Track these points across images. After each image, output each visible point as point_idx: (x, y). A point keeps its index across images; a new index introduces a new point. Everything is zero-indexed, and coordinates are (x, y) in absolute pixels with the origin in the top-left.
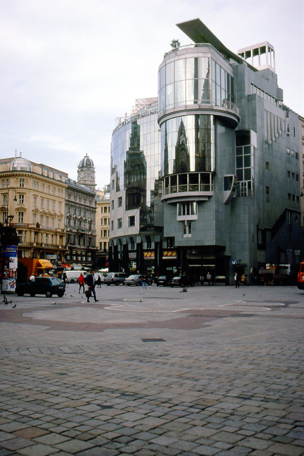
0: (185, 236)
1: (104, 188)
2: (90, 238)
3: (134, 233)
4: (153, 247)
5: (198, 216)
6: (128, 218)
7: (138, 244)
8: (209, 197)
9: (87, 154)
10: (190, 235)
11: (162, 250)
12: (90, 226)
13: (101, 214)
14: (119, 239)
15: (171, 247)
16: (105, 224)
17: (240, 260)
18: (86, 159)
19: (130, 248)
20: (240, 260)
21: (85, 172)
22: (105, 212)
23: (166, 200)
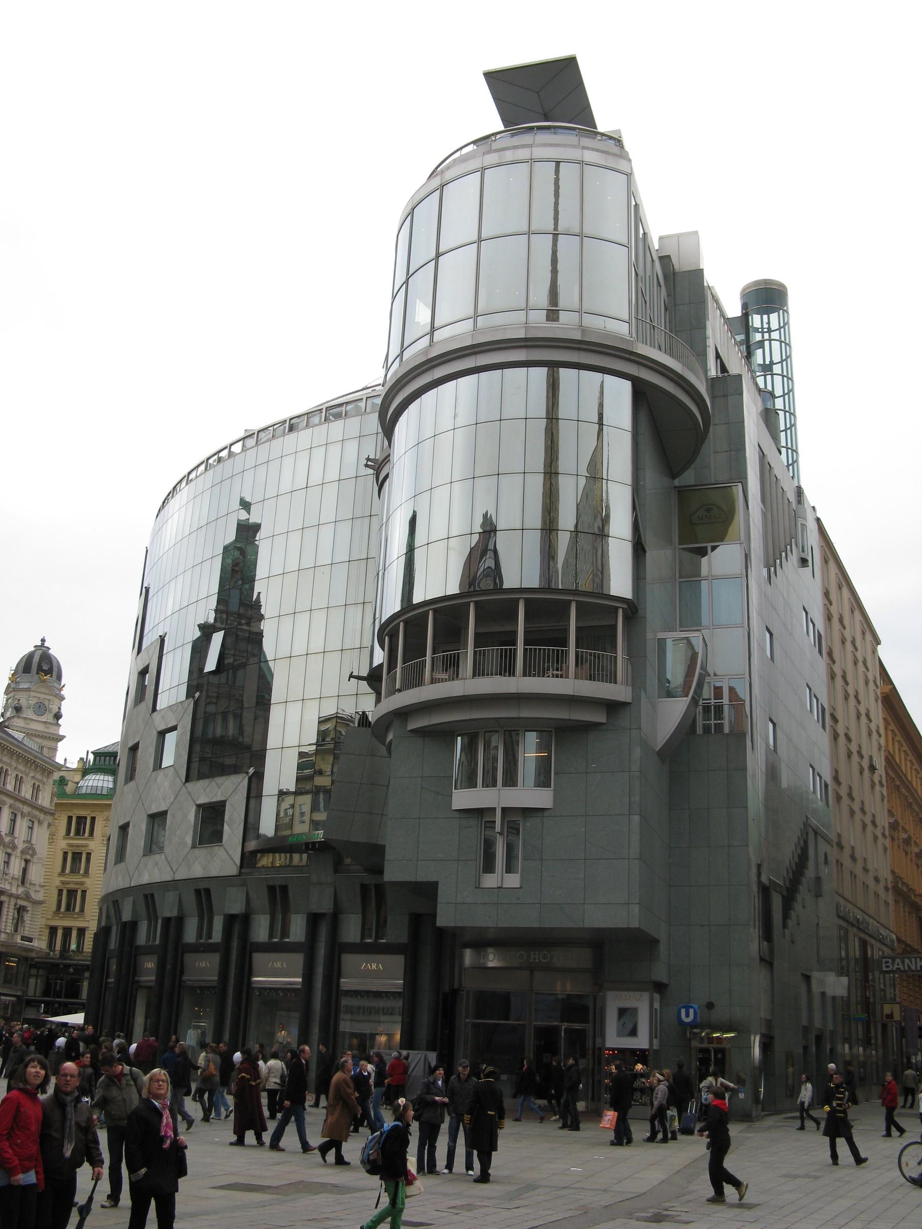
0: (490, 881)
1: (82, 759)
2: (21, 910)
3: (214, 873)
4: (298, 929)
5: (555, 791)
6: (194, 809)
7: (230, 920)
8: (613, 707)
9: (43, 640)
10: (513, 880)
11: (337, 949)
12: (25, 870)
13: (64, 838)
14: (146, 896)
15: (377, 937)
16: (75, 870)
17: (710, 1006)
18: (39, 653)
19: (190, 935)
20: (710, 1006)
21: (32, 694)
22: (78, 833)
23: (403, 714)
